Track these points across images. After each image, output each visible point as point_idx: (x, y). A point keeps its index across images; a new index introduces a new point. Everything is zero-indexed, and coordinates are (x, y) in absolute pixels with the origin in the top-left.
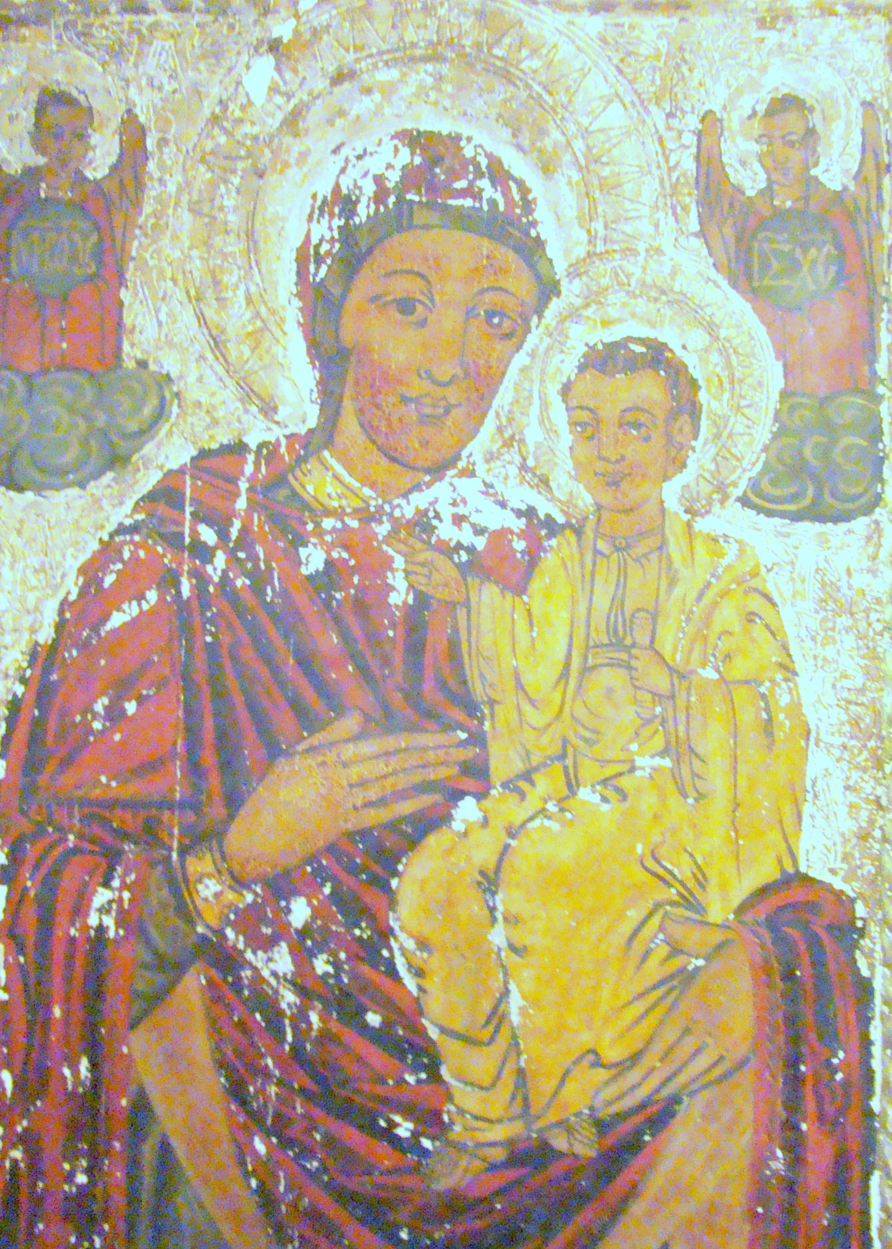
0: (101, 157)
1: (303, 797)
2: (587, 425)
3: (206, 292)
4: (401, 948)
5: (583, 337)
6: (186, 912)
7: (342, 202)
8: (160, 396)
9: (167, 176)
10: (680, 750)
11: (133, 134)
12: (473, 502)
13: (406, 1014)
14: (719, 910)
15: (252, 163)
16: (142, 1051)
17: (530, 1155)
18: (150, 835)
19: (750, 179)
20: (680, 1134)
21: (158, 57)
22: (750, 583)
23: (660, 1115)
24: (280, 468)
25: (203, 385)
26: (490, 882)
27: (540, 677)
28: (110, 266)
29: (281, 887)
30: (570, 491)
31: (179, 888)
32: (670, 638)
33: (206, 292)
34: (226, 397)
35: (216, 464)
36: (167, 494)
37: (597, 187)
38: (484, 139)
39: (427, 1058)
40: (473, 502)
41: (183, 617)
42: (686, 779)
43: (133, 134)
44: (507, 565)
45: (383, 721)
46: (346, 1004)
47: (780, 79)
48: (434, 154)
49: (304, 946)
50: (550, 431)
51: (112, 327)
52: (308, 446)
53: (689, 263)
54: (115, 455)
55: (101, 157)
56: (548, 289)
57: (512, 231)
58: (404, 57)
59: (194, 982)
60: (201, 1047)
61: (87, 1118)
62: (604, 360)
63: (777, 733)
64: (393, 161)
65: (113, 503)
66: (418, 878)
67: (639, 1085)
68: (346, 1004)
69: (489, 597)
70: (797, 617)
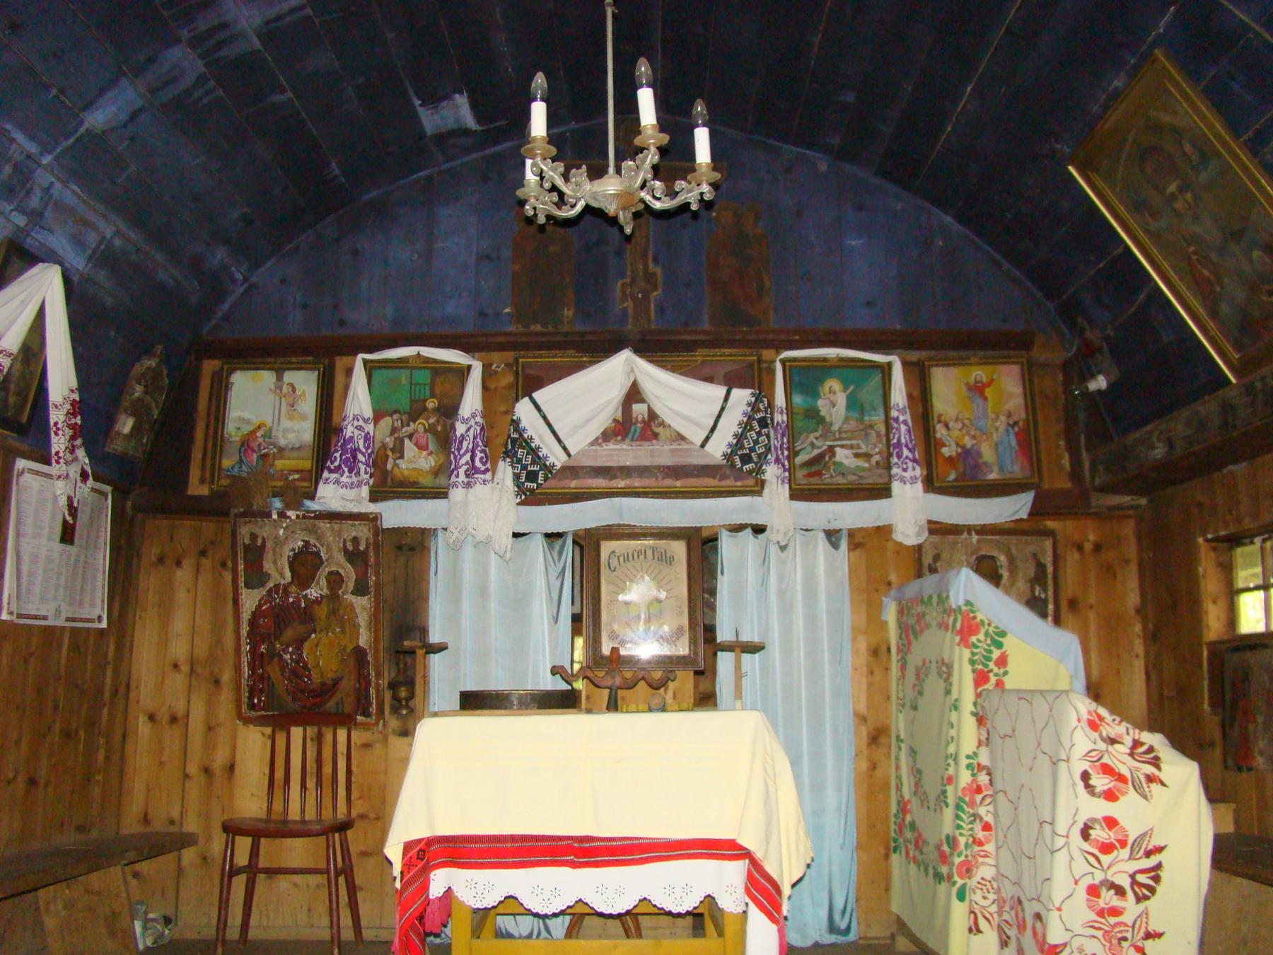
0: (259, 542)
1: (289, 634)
2: (328, 581)
3: (275, 562)
4: (305, 655)
5: (327, 570)
6: (275, 649)
7: (293, 549)
8: (268, 576)
9: (269, 545)
10: (343, 628)
11: (264, 539)
12: (313, 593)
13: (306, 664)
14: (348, 650)
15: (279, 543)
16: (269, 668)
17: (323, 684)
18: (269, 638)
19: (351, 548)
20: (345, 682)
21: (267, 528)
22: (351, 605)
23: (341, 679)
24: (286, 588)
25: (274, 574)
26: (317, 645)
27: (323, 617)
28: (261, 557)
29: (288, 647)
30: (325, 591)
31: (273, 645)
32: (341, 612)
33: (275, 562)
34: (278, 577)
35: (277, 586)
36: (270, 591)
37: (329, 550)
38: (312, 541)
39: (309, 670)
40: (313, 593)
41: (272, 608)
42: (343, 631)
43: (264, 539)
44: (317, 602)
45: (301, 623)
46: (297, 662)
47: (354, 534)
48: (307, 543)
49: (291, 654)
50: (324, 583)
51: (261, 566)
52: (290, 584)
53: (341, 557)
54: (263, 585)
55: (259, 542)
56: (322, 563)
57: (317, 554)
58: (302, 530)
59: (276, 659)
60: (277, 669)
61: (262, 678)
62: (331, 573)
63: (356, 627)
64: (300, 544)
65: (263, 591)
66: (306, 645)
67: (339, 674)
68: (297, 662)
69: (316, 607)
70: (358, 610)
